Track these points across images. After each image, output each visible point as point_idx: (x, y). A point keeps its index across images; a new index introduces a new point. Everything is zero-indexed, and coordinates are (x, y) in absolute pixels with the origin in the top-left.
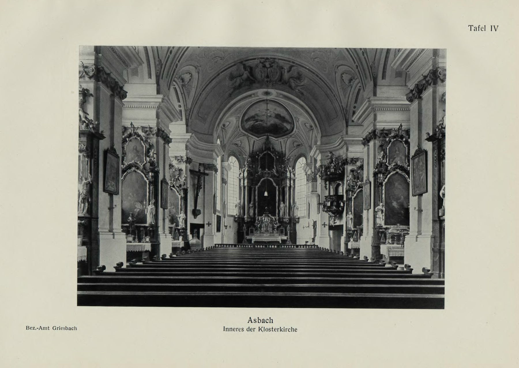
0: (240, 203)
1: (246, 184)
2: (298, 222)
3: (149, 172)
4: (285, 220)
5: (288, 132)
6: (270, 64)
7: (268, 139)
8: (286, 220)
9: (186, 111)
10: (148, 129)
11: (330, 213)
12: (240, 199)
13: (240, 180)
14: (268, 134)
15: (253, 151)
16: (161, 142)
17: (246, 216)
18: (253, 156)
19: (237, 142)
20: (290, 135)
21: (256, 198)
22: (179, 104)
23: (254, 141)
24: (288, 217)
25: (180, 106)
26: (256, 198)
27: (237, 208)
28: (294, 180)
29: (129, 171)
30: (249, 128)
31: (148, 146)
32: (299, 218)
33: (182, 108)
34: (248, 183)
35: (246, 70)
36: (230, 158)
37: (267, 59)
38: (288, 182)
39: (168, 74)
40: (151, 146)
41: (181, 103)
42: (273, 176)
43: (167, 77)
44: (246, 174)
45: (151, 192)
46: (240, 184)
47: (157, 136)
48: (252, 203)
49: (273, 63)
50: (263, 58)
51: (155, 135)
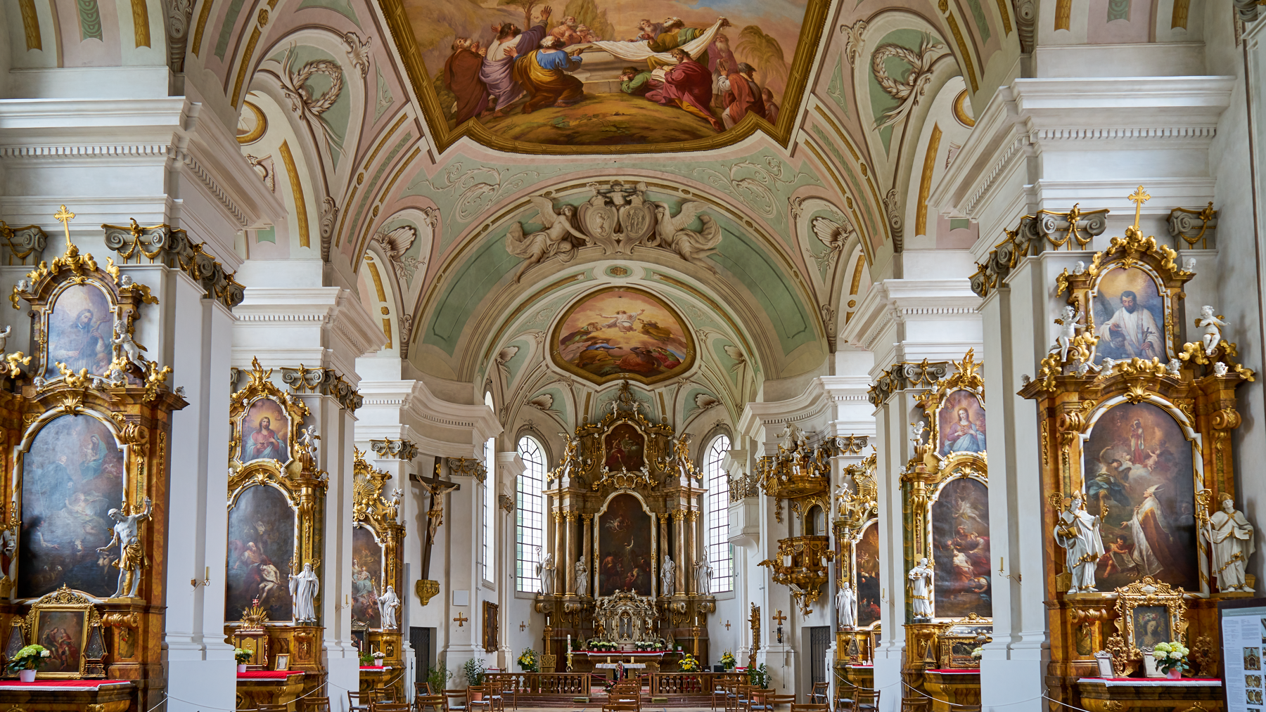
0: (550, 562)
1: (567, 510)
2: (713, 611)
3: (299, 485)
4: (674, 606)
5: (677, 369)
6: (624, 197)
7: (626, 387)
8: (680, 606)
9: (402, 322)
10: (299, 375)
11: (794, 586)
12: (551, 549)
13: (550, 499)
14: (627, 375)
15: (585, 419)
16: (334, 406)
17: (567, 596)
18: (585, 433)
19: (541, 398)
20: (687, 374)
21: (596, 546)
22: (384, 304)
23: (589, 395)
24: (683, 595)
25: (386, 311)
26: (596, 546)
27: (543, 575)
28: (700, 497)
29: (248, 483)
30: (571, 361)
31: (298, 419)
32: (714, 601)
33: (393, 317)
34: (571, 505)
35: (559, 214)
36: (523, 441)
37: (617, 183)
38: (683, 502)
39: (352, 234)
40: (306, 418)
41: (390, 304)
42: (643, 487)
43: (350, 242)
44: (566, 480)
45: (305, 535)
46: (550, 510)
47: (324, 392)
48: (583, 559)
49: (631, 194)
50: (607, 182)
51: (318, 389)
